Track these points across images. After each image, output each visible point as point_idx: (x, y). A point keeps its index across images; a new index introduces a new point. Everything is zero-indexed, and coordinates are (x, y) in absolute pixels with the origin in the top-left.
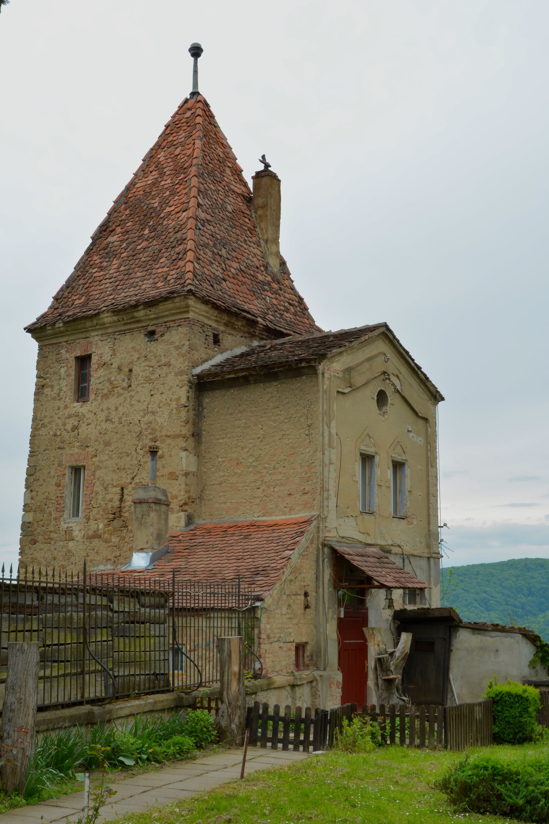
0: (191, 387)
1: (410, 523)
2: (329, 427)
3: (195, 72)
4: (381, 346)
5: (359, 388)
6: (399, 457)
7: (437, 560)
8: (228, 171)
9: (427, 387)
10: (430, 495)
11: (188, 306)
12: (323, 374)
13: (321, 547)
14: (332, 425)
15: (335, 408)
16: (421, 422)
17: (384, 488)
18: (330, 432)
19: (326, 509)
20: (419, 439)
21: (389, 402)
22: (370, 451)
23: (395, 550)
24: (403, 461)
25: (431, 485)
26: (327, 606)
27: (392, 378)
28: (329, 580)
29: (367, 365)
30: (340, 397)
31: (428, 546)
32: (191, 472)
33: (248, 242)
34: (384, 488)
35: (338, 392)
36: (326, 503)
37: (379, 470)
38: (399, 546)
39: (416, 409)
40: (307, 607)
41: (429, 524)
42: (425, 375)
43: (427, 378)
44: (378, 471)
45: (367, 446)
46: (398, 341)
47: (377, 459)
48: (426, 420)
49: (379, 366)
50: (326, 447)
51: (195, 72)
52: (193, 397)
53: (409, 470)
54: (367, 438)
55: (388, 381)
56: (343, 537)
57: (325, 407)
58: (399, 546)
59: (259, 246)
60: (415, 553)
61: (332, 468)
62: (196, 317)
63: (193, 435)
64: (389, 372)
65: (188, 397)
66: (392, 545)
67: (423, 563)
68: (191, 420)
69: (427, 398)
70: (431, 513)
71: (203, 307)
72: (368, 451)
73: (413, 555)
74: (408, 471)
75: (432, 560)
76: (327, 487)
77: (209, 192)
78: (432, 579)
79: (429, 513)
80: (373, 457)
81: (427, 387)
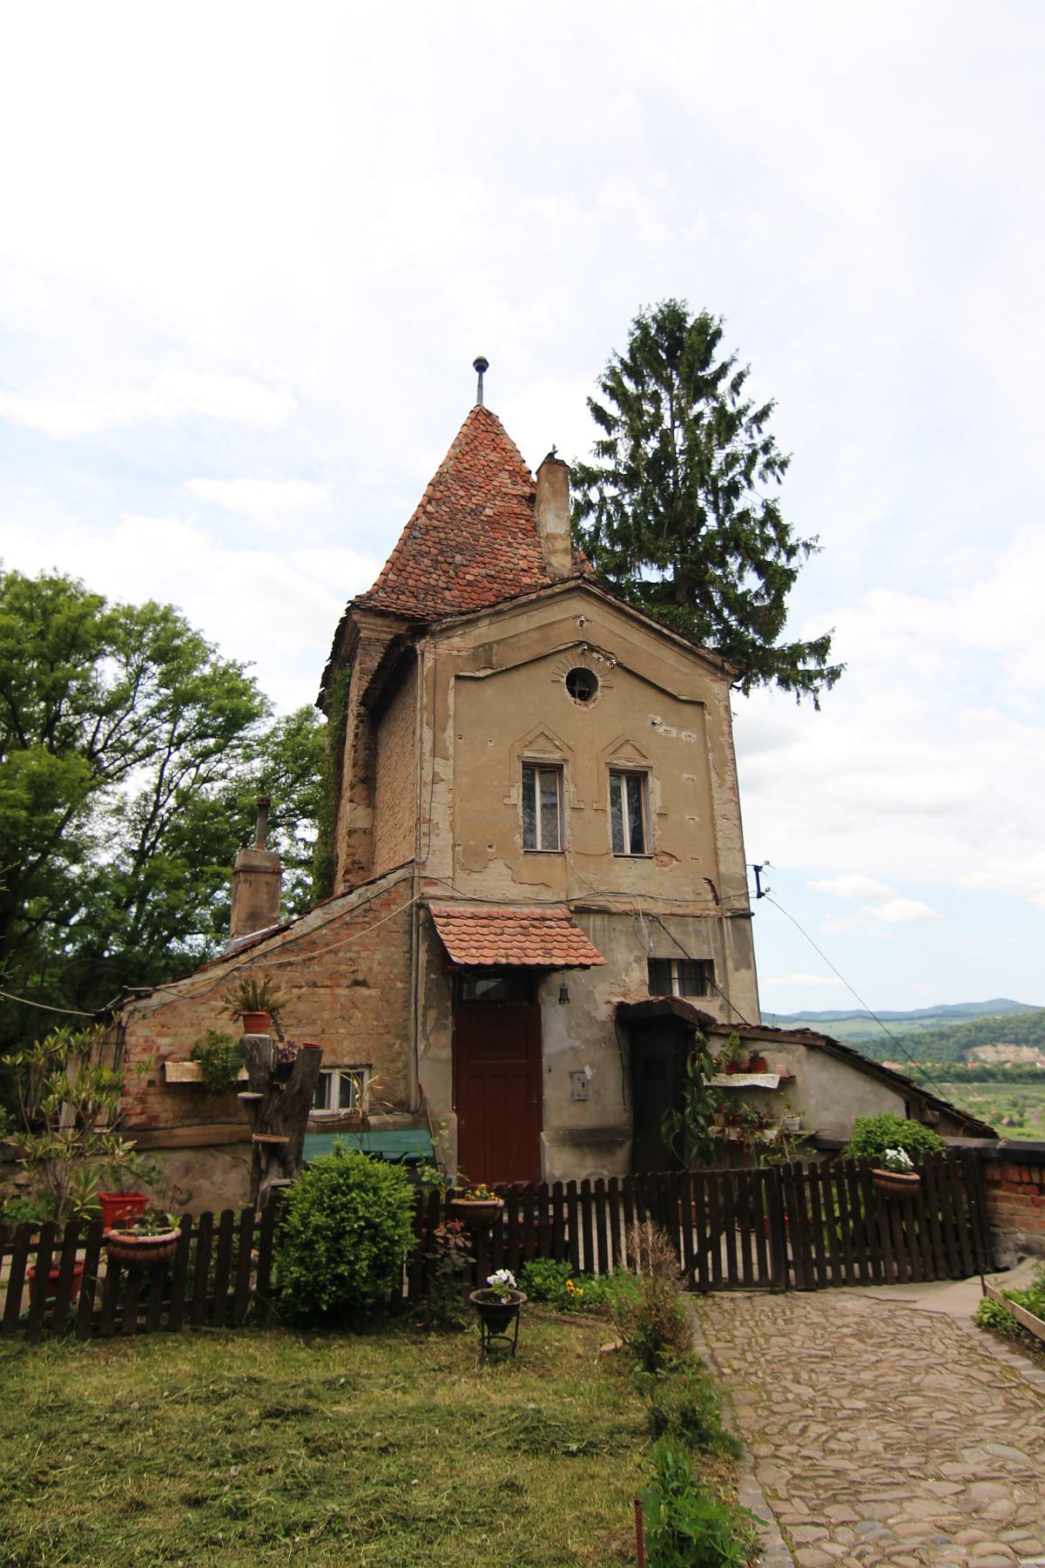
3: (480, 386)
5: (516, 667)
7: (742, 922)
8: (505, 475)
10: (717, 816)
11: (355, 623)
16: (688, 708)
17: (589, 813)
22: (553, 757)
26: (422, 1002)
29: (535, 636)
30: (470, 685)
31: (717, 900)
34: (589, 813)
35: (458, 678)
36: (424, 841)
44: (569, 787)
48: (701, 704)
50: (427, 756)
51: (480, 386)
54: (541, 740)
62: (374, 635)
63: (363, 781)
69: (700, 671)
70: (719, 845)
71: (379, 621)
74: (654, 783)
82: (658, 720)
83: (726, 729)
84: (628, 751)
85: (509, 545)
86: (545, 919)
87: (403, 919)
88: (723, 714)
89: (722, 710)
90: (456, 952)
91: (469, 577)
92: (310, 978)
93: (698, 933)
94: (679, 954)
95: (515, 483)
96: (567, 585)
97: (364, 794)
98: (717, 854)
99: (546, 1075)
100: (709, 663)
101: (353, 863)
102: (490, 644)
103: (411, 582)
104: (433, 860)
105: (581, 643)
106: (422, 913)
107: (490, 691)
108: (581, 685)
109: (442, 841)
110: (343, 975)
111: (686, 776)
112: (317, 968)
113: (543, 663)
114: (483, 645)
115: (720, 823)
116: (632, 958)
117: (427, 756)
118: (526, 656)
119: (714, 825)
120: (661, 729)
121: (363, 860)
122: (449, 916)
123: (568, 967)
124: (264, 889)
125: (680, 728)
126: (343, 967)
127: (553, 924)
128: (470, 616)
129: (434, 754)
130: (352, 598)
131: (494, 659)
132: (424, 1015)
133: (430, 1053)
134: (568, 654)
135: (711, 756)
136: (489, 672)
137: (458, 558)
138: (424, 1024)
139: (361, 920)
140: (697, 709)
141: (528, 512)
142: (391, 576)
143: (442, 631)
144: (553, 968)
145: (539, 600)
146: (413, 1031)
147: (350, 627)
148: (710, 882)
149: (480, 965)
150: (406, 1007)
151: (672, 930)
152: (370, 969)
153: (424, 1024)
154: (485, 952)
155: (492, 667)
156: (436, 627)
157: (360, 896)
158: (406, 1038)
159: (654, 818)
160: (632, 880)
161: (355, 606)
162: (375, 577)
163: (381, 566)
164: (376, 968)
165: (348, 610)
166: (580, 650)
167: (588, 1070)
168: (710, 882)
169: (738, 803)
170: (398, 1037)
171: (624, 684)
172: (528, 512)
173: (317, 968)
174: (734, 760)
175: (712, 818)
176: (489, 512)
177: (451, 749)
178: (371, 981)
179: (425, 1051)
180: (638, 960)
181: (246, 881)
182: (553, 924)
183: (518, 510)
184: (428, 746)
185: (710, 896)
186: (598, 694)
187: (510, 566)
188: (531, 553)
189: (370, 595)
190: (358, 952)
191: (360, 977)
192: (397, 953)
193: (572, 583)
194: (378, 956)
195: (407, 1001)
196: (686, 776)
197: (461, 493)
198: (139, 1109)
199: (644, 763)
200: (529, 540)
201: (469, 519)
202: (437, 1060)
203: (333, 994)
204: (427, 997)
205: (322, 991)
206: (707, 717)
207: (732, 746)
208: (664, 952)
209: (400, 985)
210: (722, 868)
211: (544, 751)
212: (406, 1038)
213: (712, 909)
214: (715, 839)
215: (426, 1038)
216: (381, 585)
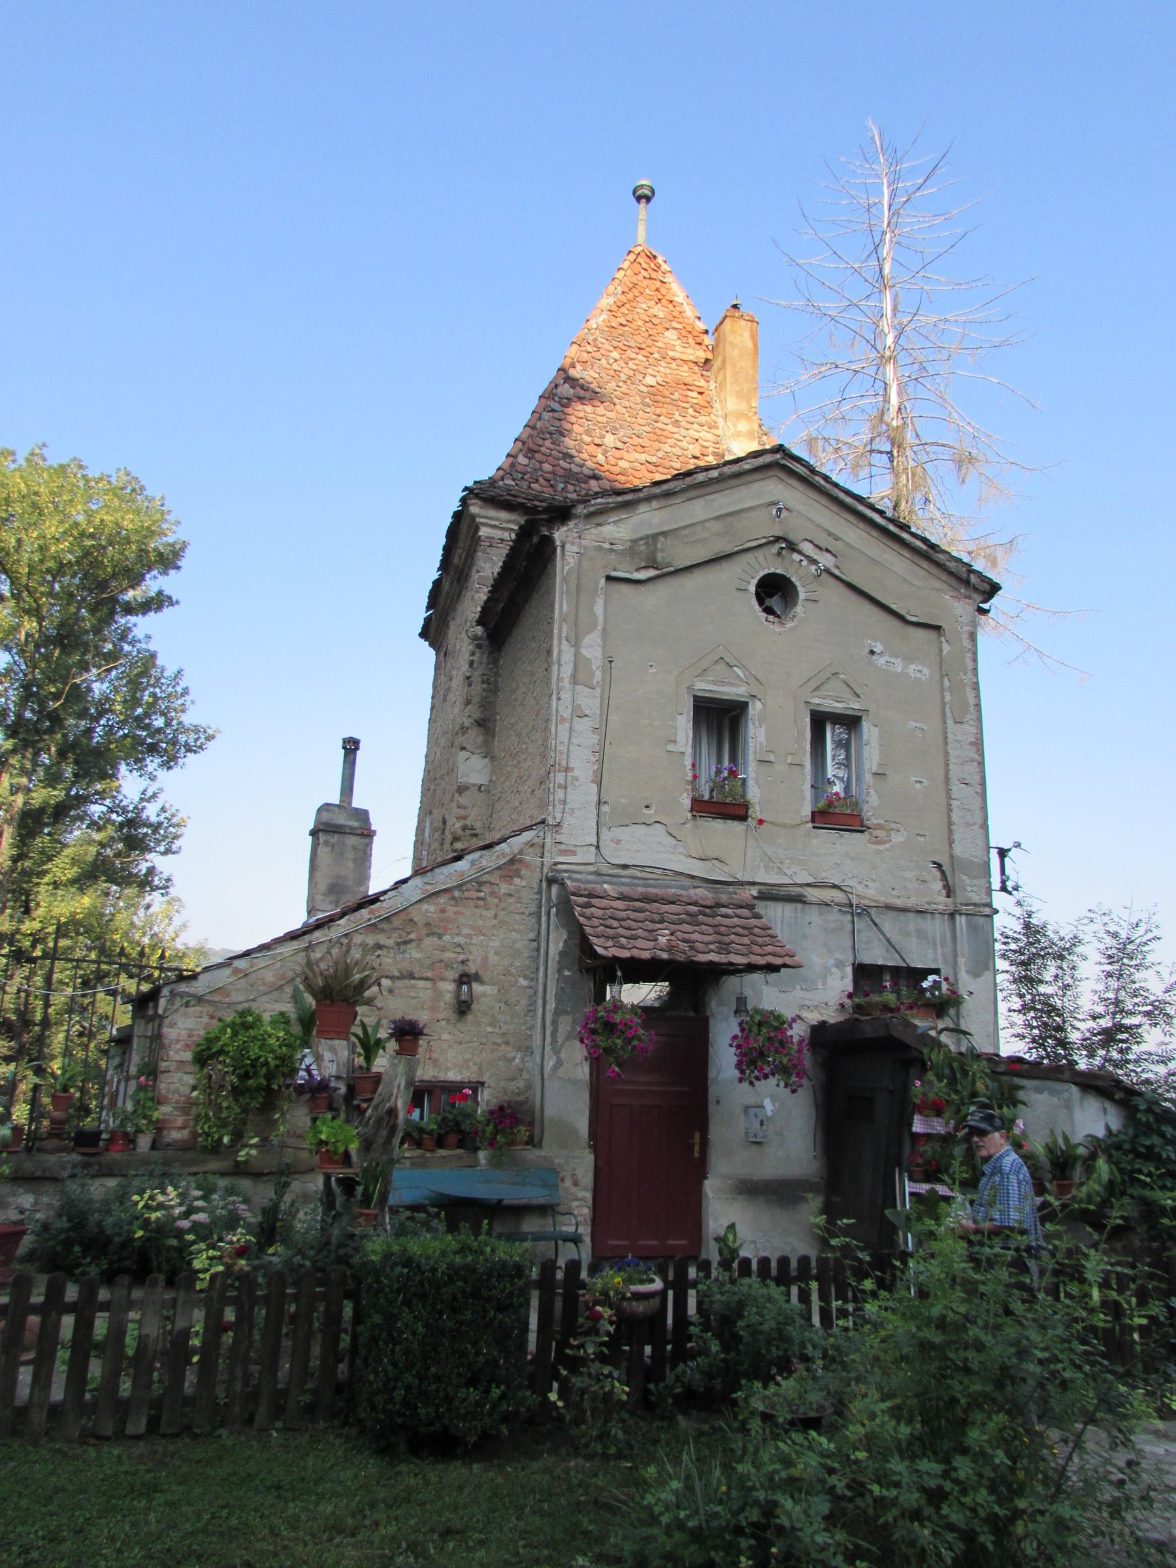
0: (479, 646)
1: (878, 841)
2: (576, 645)
4: (775, 489)
6: (840, 705)
8: (671, 335)
9: (938, 565)
10: (953, 780)
11: (473, 517)
12: (563, 547)
13: (544, 884)
14: (586, 641)
15: (599, 609)
18: (577, 654)
19: (559, 807)
20: (913, 667)
21: (802, 596)
23: (813, 894)
24: (850, 713)
25: (952, 760)
26: (551, 1005)
27: (807, 548)
28: (562, 954)
29: (716, 527)
30: (624, 588)
32: (474, 785)
33: (684, 424)
34: (780, 768)
35: (609, 578)
37: (762, 731)
38: (835, 886)
39: (894, 607)
40: (463, 1008)
41: (951, 843)
42: (925, 540)
43: (933, 547)
45: (714, 682)
46: (826, 478)
47: (755, 709)
48: (938, 628)
49: (761, 527)
50: (566, 683)
52: (484, 661)
53: (875, 732)
54: (721, 667)
55: (796, 557)
56: (625, 867)
57: (565, 607)
58: (835, 886)
59: (713, 426)
60: (899, 902)
61: (583, 726)
62: (498, 534)
64: (792, 537)
65: (471, 663)
66: (808, 885)
67: (936, 927)
68: (475, 700)
69: (937, 584)
70: (955, 818)
72: (729, 694)
73: (889, 908)
74: (868, 730)
75: (961, 921)
76: (564, 764)
77: (604, 361)
78: (961, 961)
79: (949, 817)
80: (746, 704)
81: (938, 565)
82: (878, 648)
83: (970, 664)
84: (835, 687)
85: (676, 423)
86: (719, 905)
87: (529, 896)
88: (966, 643)
89: (965, 636)
90: (601, 941)
91: (622, 464)
92: (406, 966)
93: (920, 934)
94: (893, 961)
95: (686, 345)
96: (761, 461)
97: (480, 739)
98: (950, 831)
99: (712, 1108)
100: (951, 573)
101: (464, 828)
102: (655, 537)
103: (547, 467)
104: (569, 821)
105: (778, 539)
106: (555, 889)
107: (655, 598)
108: (774, 592)
109: (582, 795)
110: (448, 966)
111: (914, 724)
112: (415, 954)
113: (725, 565)
114: (646, 537)
115: (957, 789)
116: (831, 962)
117: (566, 683)
118: (702, 554)
119: (948, 790)
120: (882, 661)
121: (478, 825)
122: (591, 895)
123: (751, 968)
124: (350, 855)
125: (908, 659)
126: (448, 955)
127: (729, 911)
128: (629, 497)
129: (575, 680)
130: (470, 484)
131: (659, 556)
132: (554, 1023)
133: (561, 1072)
134: (759, 554)
135: (948, 698)
136: (652, 573)
137: (610, 440)
138: (554, 1033)
139: (474, 894)
140: (932, 635)
141: (702, 383)
142: (522, 460)
143: (590, 516)
144: (732, 970)
145: (721, 479)
146: (539, 1042)
147: (464, 526)
148: (939, 866)
149: (632, 959)
150: (531, 1010)
151: (887, 927)
152: (485, 960)
153: (554, 1033)
154: (641, 943)
155: (654, 565)
156: (580, 510)
157: (473, 863)
158: (528, 1051)
159: (868, 778)
160: (835, 858)
161: (472, 493)
162: (500, 460)
163: (508, 446)
164: (493, 959)
165: (463, 501)
166: (776, 547)
167: (768, 1103)
168: (939, 866)
169: (981, 764)
170: (519, 1049)
171: (834, 594)
172: (702, 383)
173: (415, 954)
174: (978, 706)
175: (947, 779)
176: (650, 380)
177: (598, 675)
178: (485, 976)
179: (556, 1067)
180: (839, 965)
181: (326, 843)
182: (729, 911)
183: (689, 380)
184: (567, 670)
185: (938, 885)
186: (799, 609)
187: (677, 451)
188: (704, 435)
189: (492, 482)
190: (469, 936)
191: (472, 968)
192: (520, 940)
193: (768, 459)
194: (495, 943)
195: (533, 1003)
196: (914, 724)
197: (615, 355)
198: (180, 1121)
199: (856, 706)
200: (702, 419)
201: (624, 388)
202: (574, 1082)
203: (435, 989)
204: (559, 999)
205: (421, 984)
206: (946, 648)
207: (976, 687)
208: (876, 956)
209: (523, 982)
210: (958, 850)
211: (723, 683)
212: (528, 1051)
213: (942, 902)
214: (949, 809)
215: (557, 1052)
216: (510, 468)
